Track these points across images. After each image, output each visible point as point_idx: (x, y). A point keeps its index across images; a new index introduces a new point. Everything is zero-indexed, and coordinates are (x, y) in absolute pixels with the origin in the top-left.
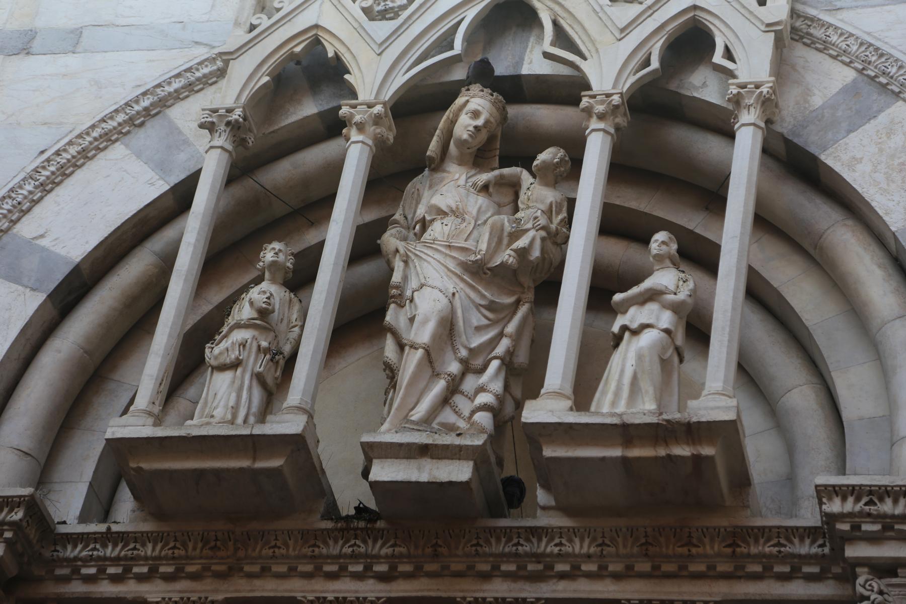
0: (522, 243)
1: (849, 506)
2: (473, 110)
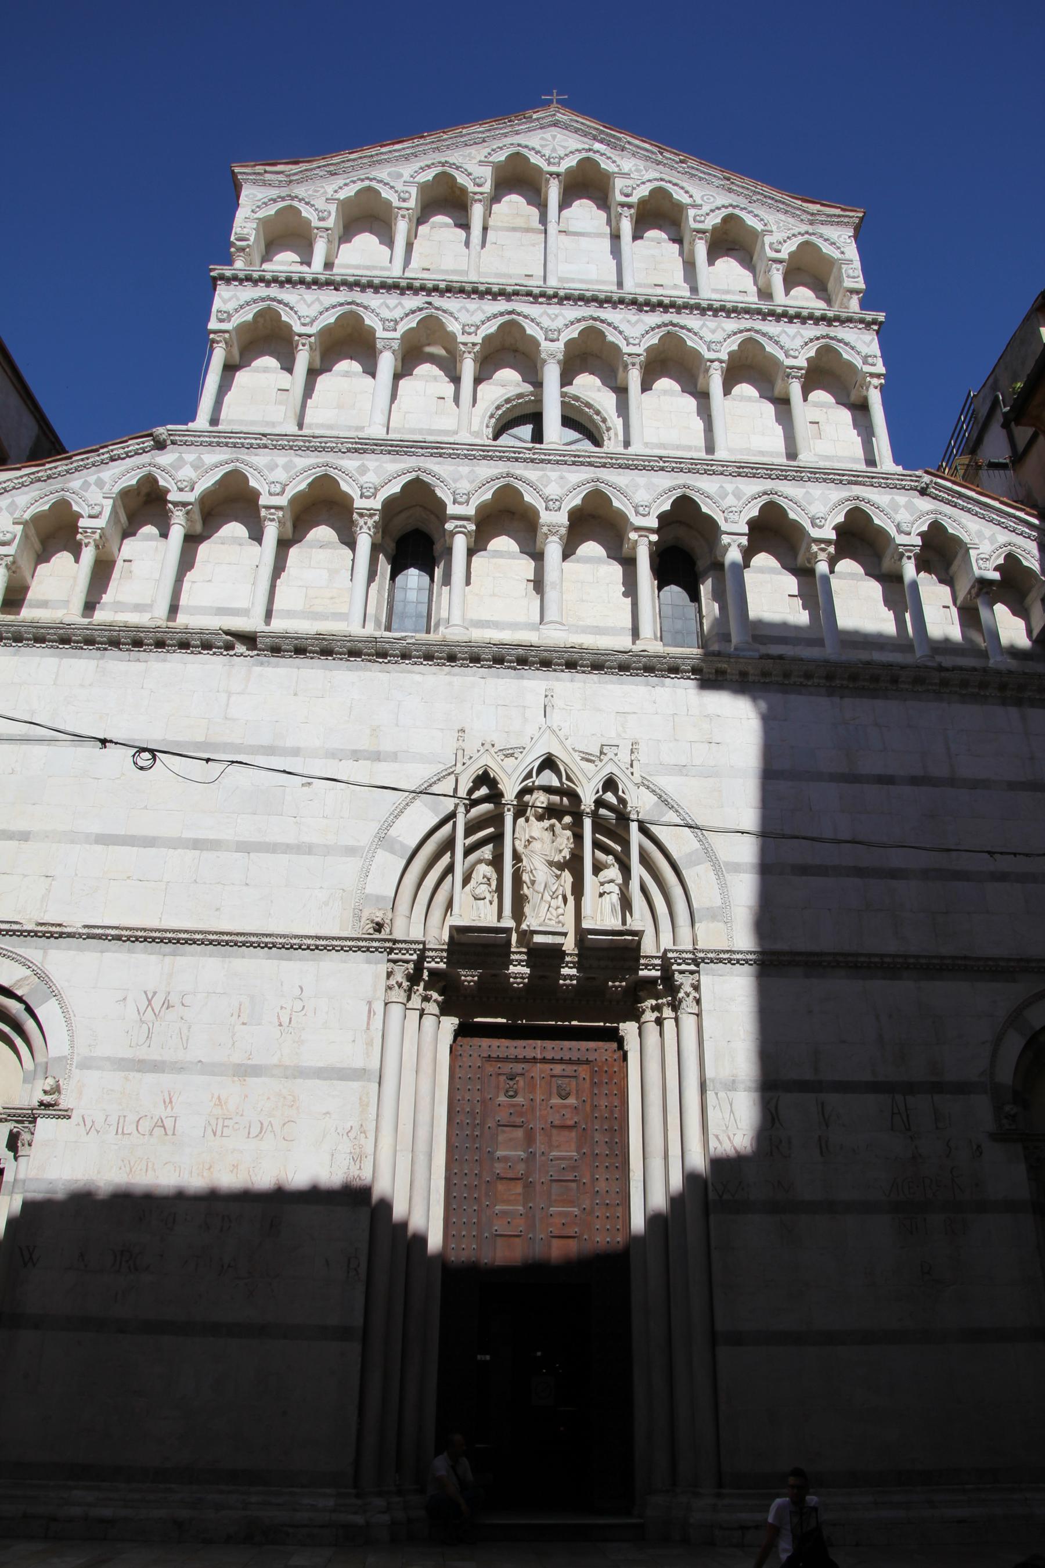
0: (563, 854)
1: (675, 955)
2: (541, 799)
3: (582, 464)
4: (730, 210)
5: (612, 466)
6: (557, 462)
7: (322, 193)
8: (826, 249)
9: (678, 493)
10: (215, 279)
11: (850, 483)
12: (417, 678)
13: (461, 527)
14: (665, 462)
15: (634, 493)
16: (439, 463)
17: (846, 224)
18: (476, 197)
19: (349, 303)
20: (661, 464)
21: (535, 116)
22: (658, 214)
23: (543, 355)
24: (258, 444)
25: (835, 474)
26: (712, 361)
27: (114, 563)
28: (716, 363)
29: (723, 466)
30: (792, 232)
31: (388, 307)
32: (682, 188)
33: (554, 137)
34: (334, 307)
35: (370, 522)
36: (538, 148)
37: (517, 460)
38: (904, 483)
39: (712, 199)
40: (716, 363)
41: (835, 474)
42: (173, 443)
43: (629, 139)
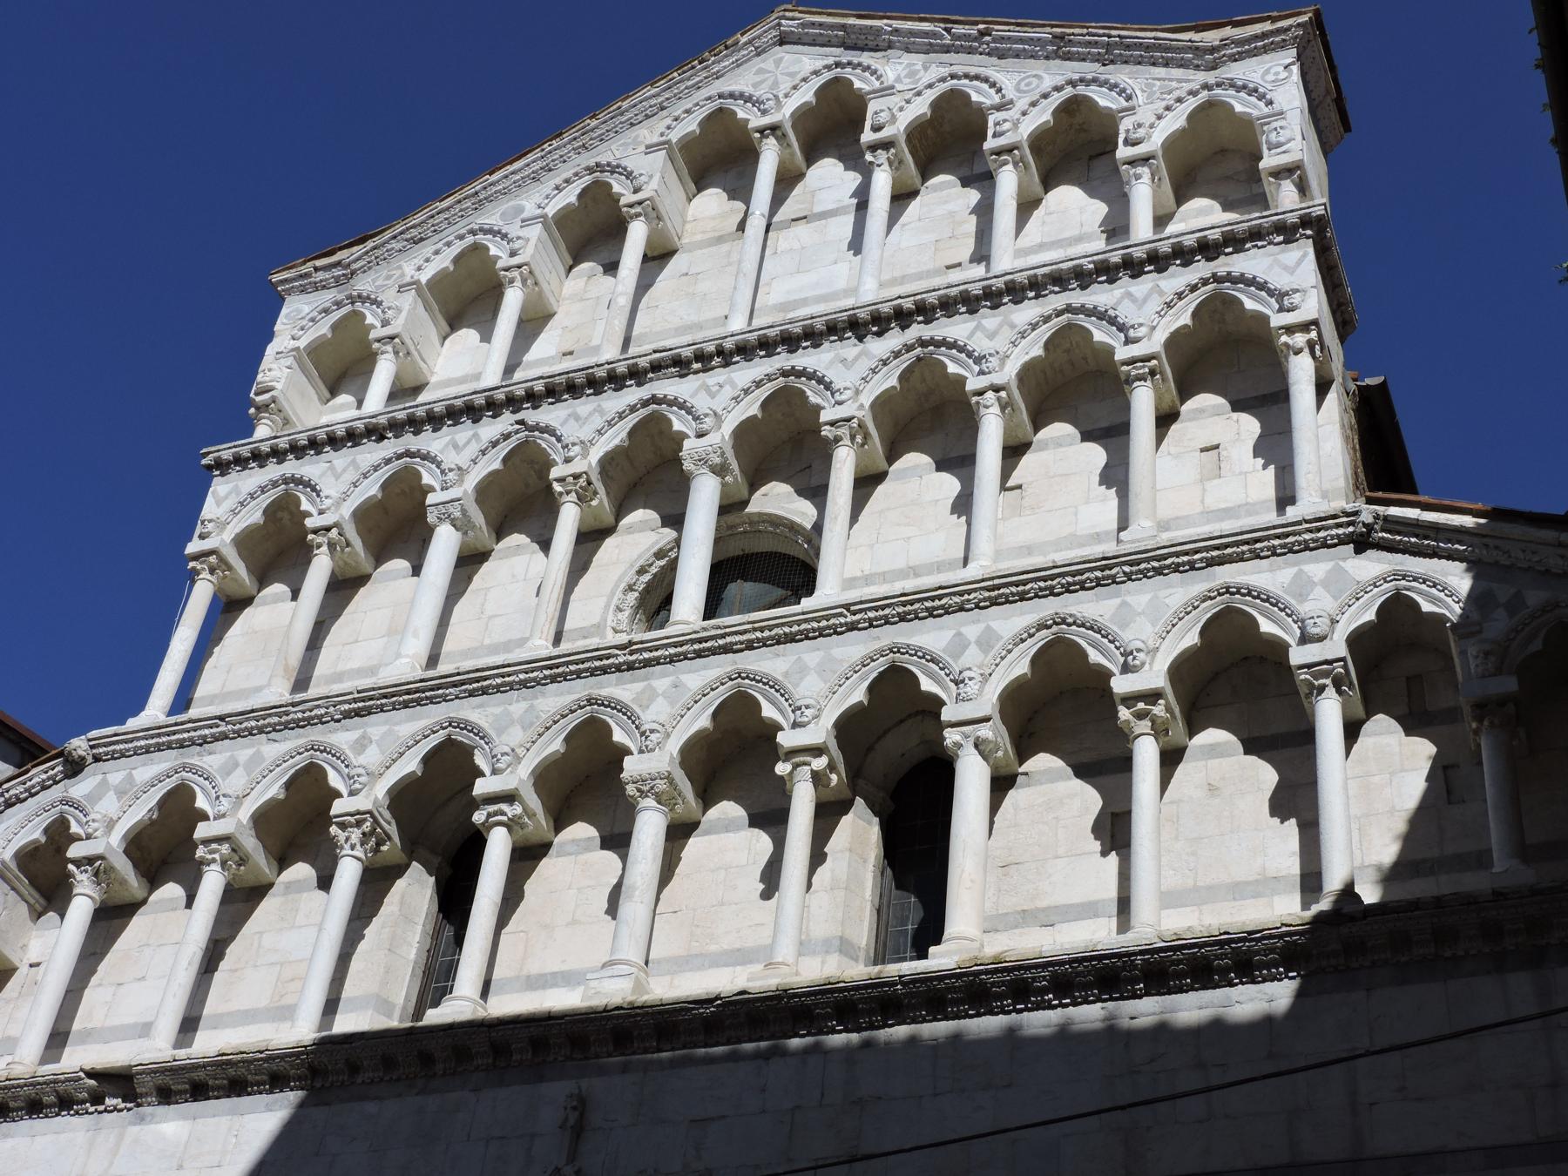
3: (714, 652)
4: (1069, 91)
5: (764, 643)
6: (672, 660)
7: (397, 279)
8: (1241, 105)
9: (880, 665)
10: (209, 468)
11: (1211, 563)
12: (371, 1107)
13: (496, 814)
14: (854, 614)
15: (797, 685)
16: (480, 706)
17: (1282, 46)
18: (633, 211)
19: (399, 457)
20: (850, 618)
21: (744, 39)
22: (950, 141)
23: (687, 465)
24: (213, 736)
25: (1177, 554)
26: (980, 393)
27: (14, 970)
28: (990, 394)
29: (961, 594)
30: (1176, 94)
31: (456, 446)
32: (986, 80)
33: (778, 62)
34: (1034, 327)
35: (356, 835)
36: (748, 90)
37: (604, 671)
38: (1322, 534)
39: (1035, 81)
40: (990, 394)
41: (1177, 554)
42: (97, 759)
43: (897, 24)
